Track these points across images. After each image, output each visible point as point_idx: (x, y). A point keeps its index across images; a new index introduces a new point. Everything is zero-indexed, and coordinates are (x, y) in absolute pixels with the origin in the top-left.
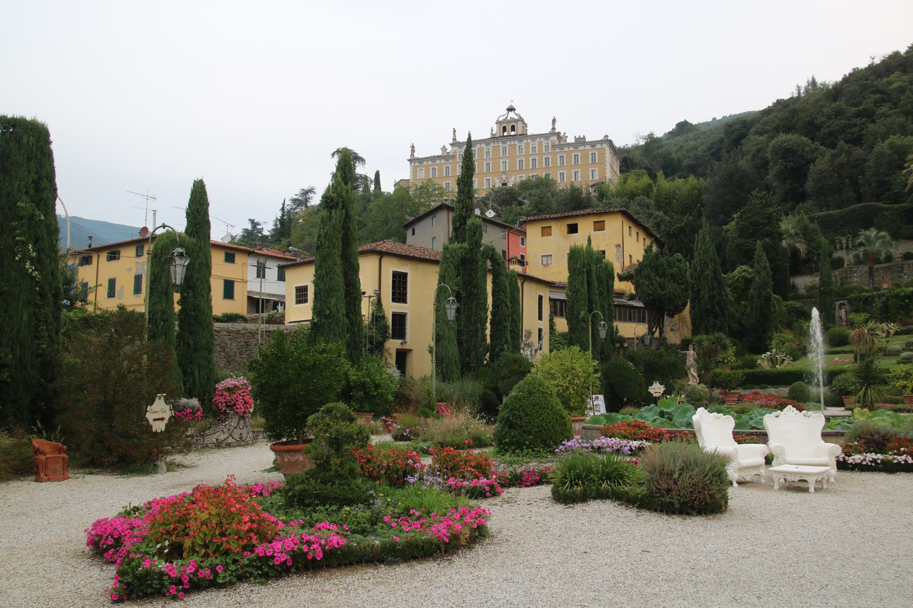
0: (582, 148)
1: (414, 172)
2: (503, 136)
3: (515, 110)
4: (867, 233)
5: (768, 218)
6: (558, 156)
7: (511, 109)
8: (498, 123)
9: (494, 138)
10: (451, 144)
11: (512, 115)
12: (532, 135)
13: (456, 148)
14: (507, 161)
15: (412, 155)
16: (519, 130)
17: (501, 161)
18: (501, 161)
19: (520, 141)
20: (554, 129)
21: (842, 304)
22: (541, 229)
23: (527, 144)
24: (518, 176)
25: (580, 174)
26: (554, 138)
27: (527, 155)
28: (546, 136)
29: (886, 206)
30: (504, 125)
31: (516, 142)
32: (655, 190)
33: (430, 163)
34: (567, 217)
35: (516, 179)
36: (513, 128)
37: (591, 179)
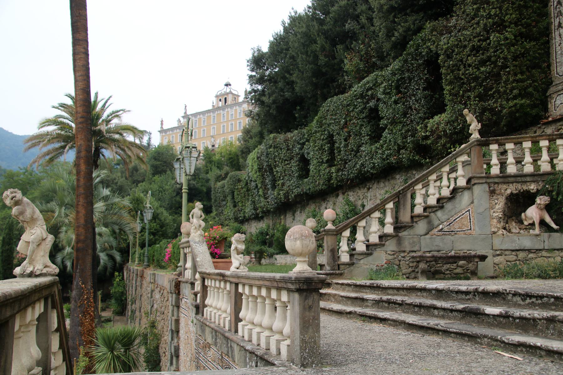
3: (230, 85)
7: (227, 85)
8: (217, 96)
9: (215, 109)
10: (183, 117)
14: (215, 127)
15: (162, 127)
17: (212, 127)
18: (212, 127)
23: (228, 112)
24: (222, 138)
27: (228, 121)
30: (220, 98)
31: (221, 111)
33: (171, 133)
35: (220, 140)
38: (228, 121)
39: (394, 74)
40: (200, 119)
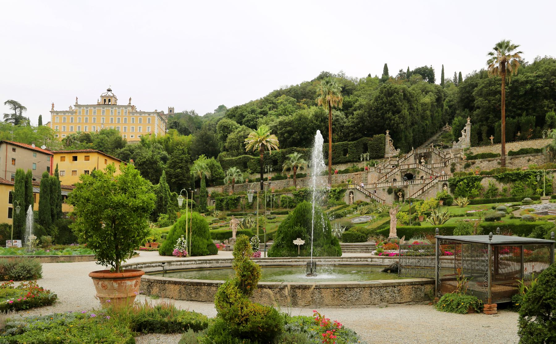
0: (143, 115)
1: (53, 118)
2: (109, 104)
4: (231, 169)
5: (181, 160)
6: (131, 118)
7: (109, 90)
8: (102, 97)
9: (99, 105)
11: (109, 93)
12: (119, 106)
13: (77, 108)
15: (53, 109)
16: (112, 102)
19: (112, 108)
20: (130, 103)
21: (214, 201)
22: (60, 158)
25: (142, 128)
26: (130, 109)
27: (115, 116)
28: (126, 107)
29: (253, 157)
31: (110, 108)
32: (171, 141)
34: (73, 152)
36: (109, 101)
37: (147, 131)
38: (115, 116)
39: (354, 143)
40: (91, 110)
